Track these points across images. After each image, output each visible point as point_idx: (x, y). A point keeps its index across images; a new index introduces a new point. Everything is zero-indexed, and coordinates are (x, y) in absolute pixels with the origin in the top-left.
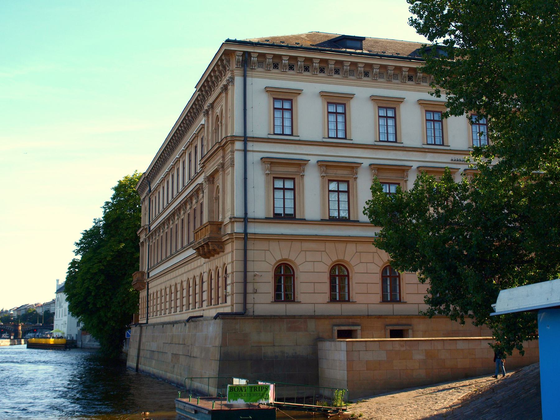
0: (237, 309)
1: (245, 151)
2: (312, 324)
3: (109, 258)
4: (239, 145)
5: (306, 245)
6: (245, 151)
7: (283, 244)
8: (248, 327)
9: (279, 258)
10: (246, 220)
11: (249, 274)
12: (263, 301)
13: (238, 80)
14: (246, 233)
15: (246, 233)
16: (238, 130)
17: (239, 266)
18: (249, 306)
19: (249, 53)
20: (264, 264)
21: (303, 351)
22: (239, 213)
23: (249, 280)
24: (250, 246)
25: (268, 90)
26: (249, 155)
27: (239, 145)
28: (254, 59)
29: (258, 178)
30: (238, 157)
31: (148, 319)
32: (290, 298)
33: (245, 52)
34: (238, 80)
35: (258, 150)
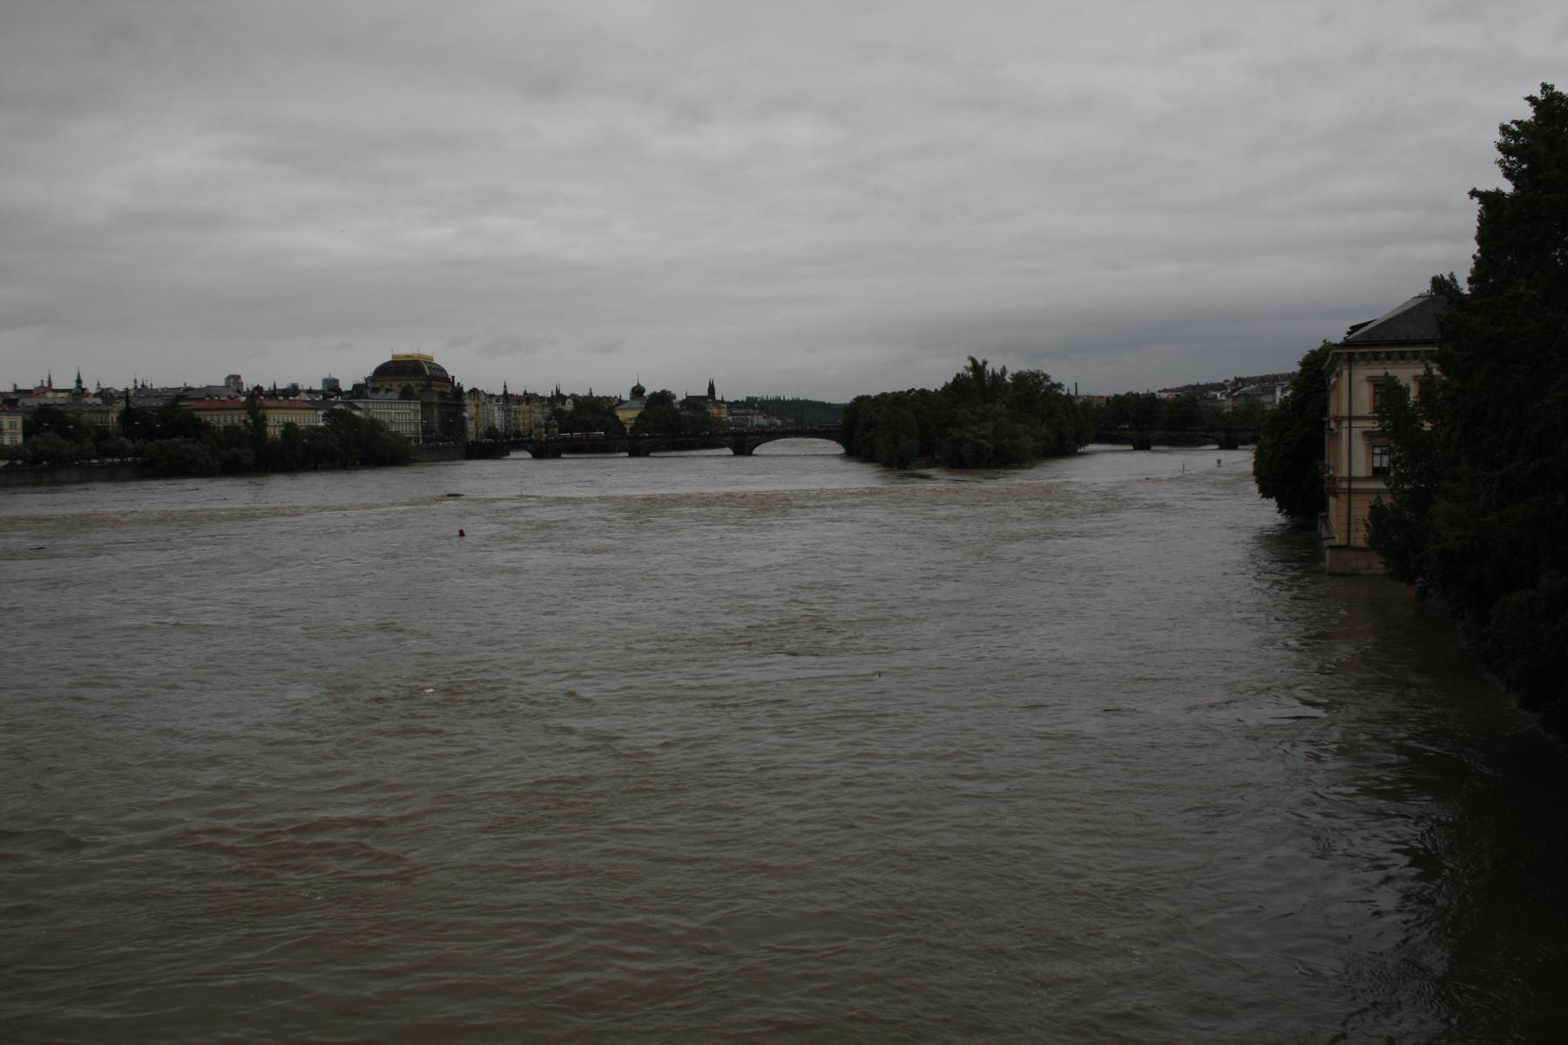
0: (1344, 542)
13: (1345, 373)
25: (1370, 379)
30: (1345, 433)
34: (1345, 373)
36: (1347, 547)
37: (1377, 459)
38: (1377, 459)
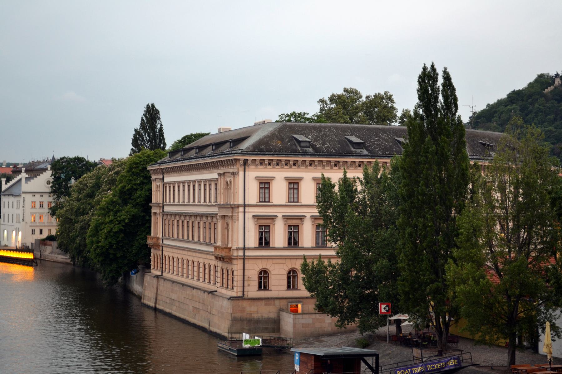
0: (240, 294)
1: (244, 212)
2: (277, 302)
3: (127, 221)
4: (241, 209)
5: (275, 261)
6: (244, 212)
7: (263, 260)
8: (245, 304)
9: (261, 267)
10: (244, 249)
11: (245, 277)
12: (253, 291)
13: (241, 173)
14: (244, 256)
15: (244, 256)
16: (241, 202)
17: (241, 273)
18: (245, 293)
19: (247, 160)
20: (253, 271)
21: (273, 315)
22: (241, 245)
23: (245, 279)
24: (246, 262)
25: (257, 178)
26: (246, 214)
27: (241, 209)
28: (250, 162)
30: (241, 216)
31: (162, 272)
32: (266, 288)
33: (245, 159)
34: (241, 173)
35: (251, 212)
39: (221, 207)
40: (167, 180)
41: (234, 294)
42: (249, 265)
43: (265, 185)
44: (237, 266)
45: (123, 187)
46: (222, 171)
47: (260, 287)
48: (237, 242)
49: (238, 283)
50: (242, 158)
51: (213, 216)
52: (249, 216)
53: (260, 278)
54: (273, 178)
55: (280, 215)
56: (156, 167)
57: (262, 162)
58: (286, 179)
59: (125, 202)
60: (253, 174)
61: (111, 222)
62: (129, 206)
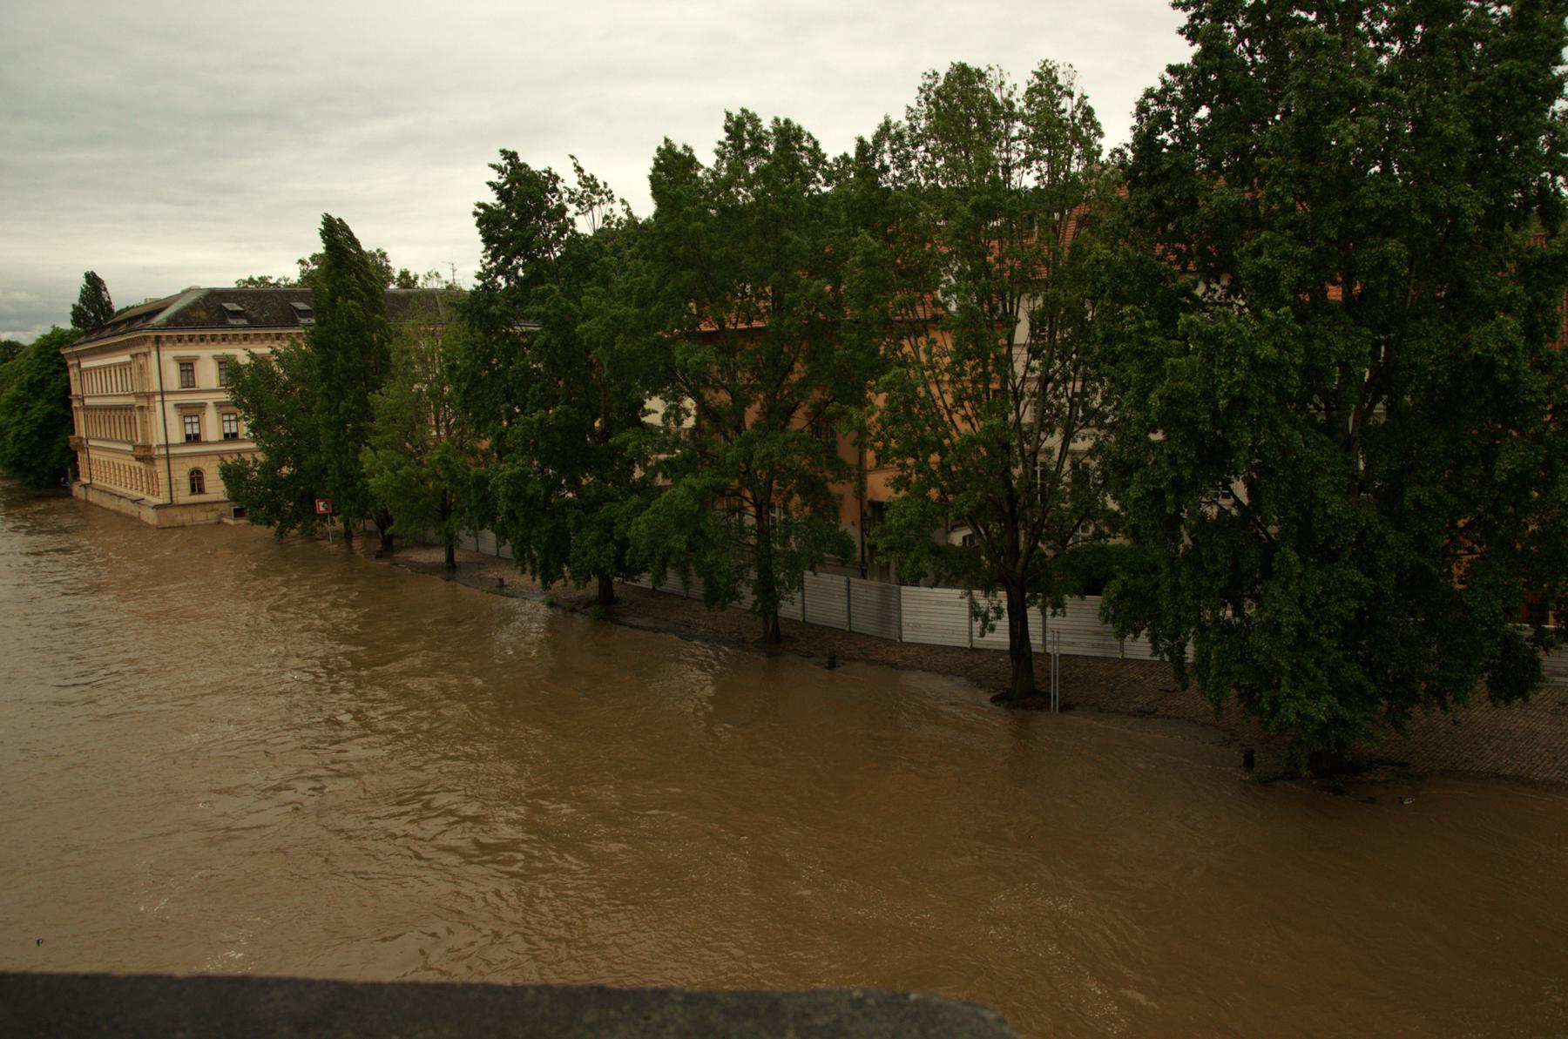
4: (158, 398)
8: (174, 512)
10: (167, 446)
12: (184, 495)
16: (156, 388)
20: (182, 473)
22: (162, 441)
25: (176, 359)
29: (173, 418)
30: (159, 406)
34: (154, 354)
35: (171, 400)
36: (171, 505)
37: (189, 427)
38: (189, 427)
39: (137, 396)
40: (84, 365)
41: (159, 501)
42: (175, 464)
43: (187, 366)
44: (161, 467)
45: (31, 379)
46: (134, 351)
47: (193, 491)
48: (157, 439)
49: (164, 488)
50: (153, 334)
51: (129, 408)
52: (169, 406)
53: (192, 480)
54: (197, 358)
55: (210, 403)
56: (69, 350)
57: (180, 339)
58: (215, 357)
59: (37, 396)
60: (170, 354)
61: (18, 423)
62: (42, 401)
